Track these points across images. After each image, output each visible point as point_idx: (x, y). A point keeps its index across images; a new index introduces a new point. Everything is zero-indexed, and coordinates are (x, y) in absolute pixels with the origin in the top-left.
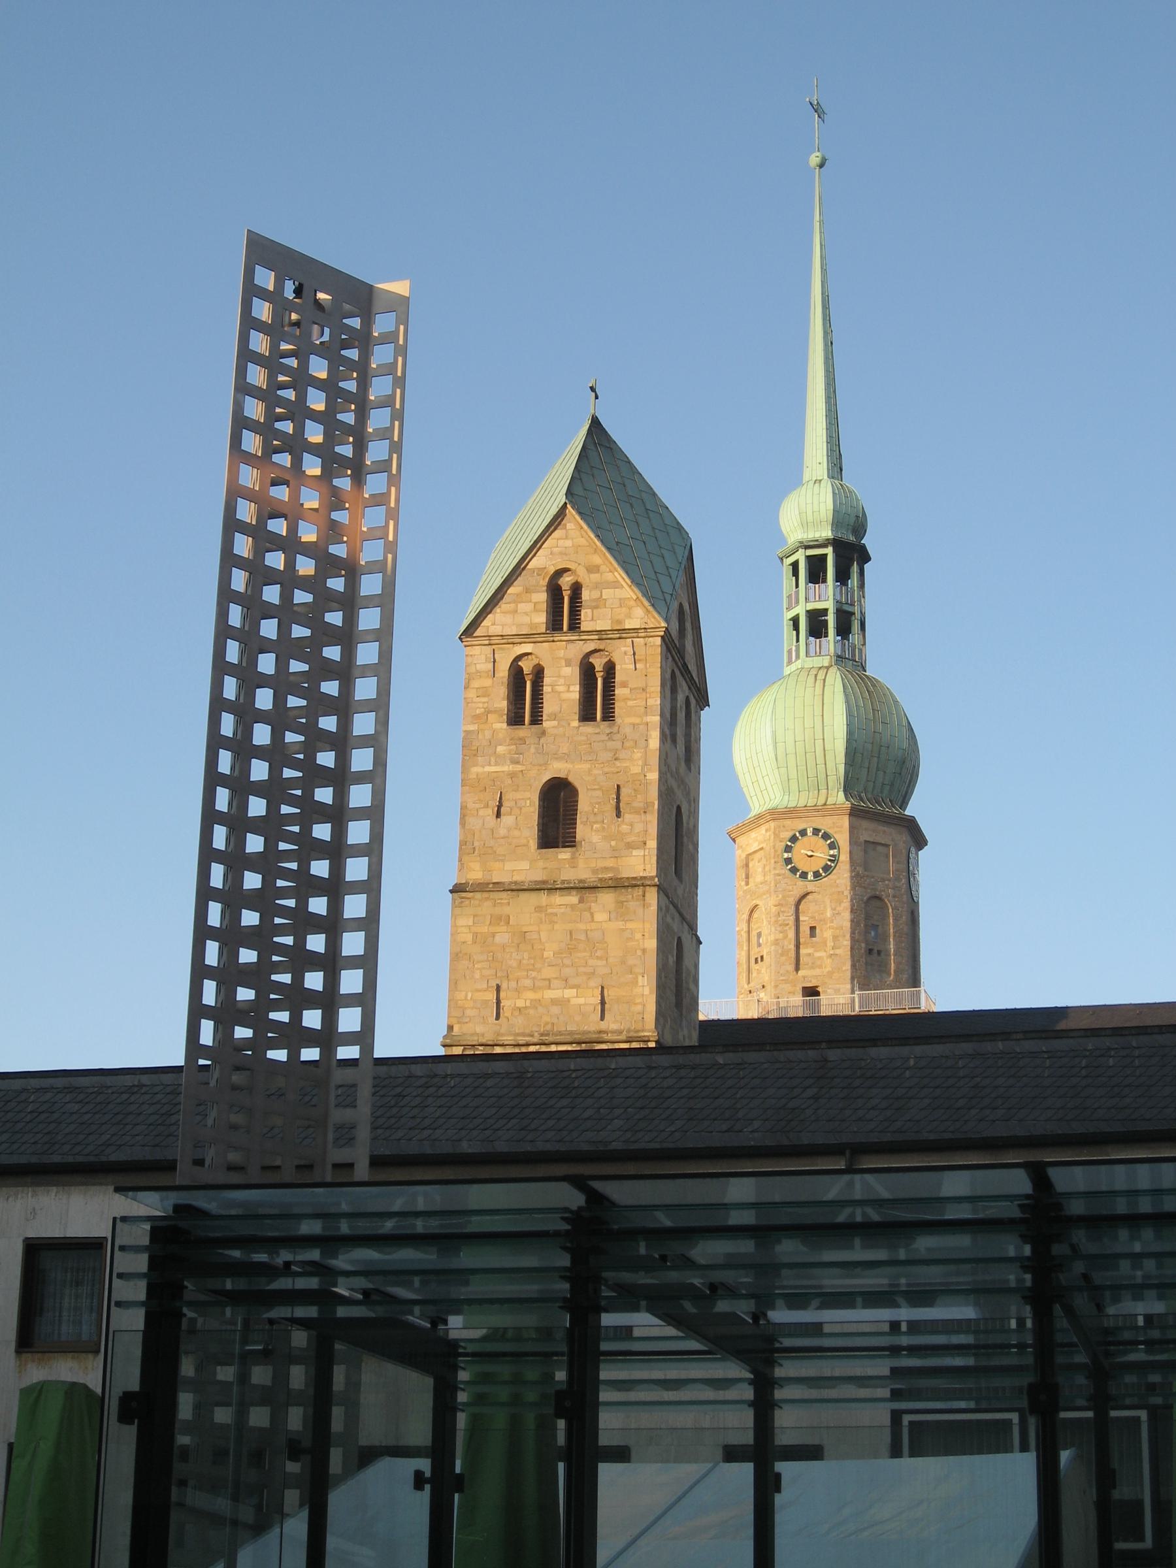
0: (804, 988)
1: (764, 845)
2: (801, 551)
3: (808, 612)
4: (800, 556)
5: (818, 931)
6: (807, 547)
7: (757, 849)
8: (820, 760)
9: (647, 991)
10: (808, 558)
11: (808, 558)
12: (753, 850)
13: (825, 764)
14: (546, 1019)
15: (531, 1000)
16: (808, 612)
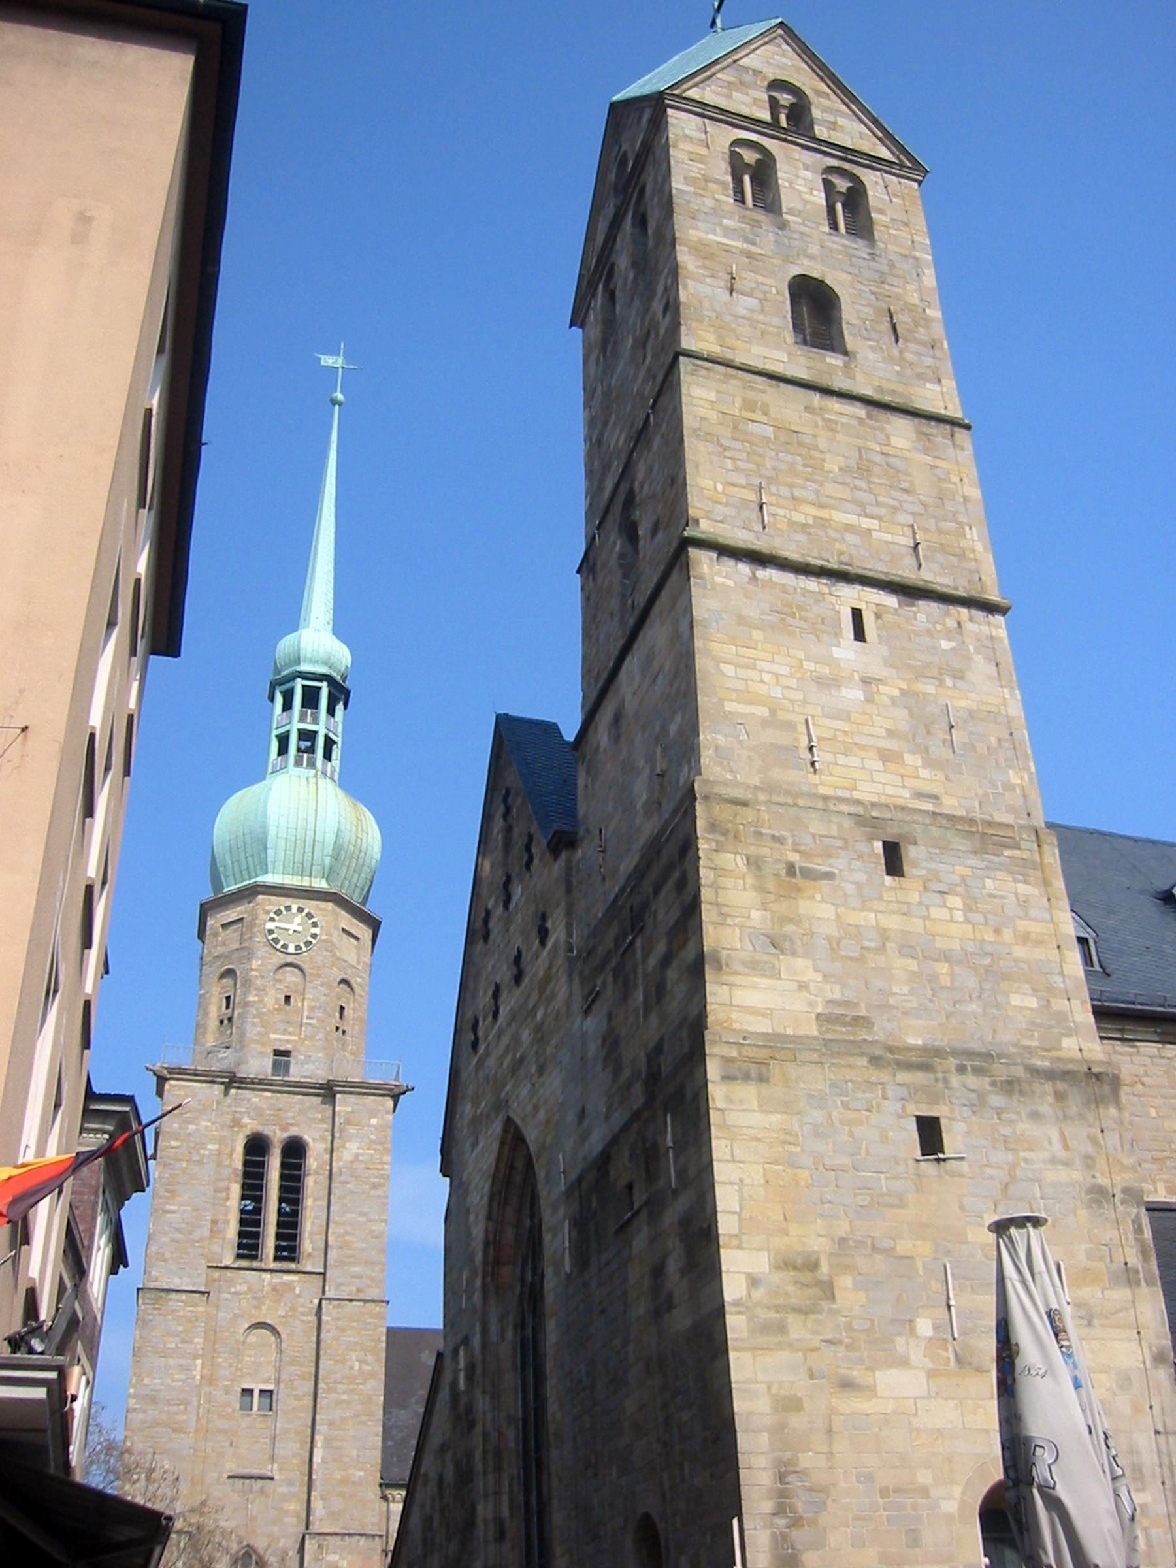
0: (275, 1051)
1: (245, 916)
2: (299, 680)
3: (299, 730)
4: (299, 684)
5: (292, 1000)
6: (304, 678)
7: (235, 918)
8: (308, 849)
9: (979, 547)
10: (304, 686)
11: (304, 686)
12: (229, 920)
13: (313, 853)
14: (838, 546)
15: (815, 518)
16: (299, 730)
